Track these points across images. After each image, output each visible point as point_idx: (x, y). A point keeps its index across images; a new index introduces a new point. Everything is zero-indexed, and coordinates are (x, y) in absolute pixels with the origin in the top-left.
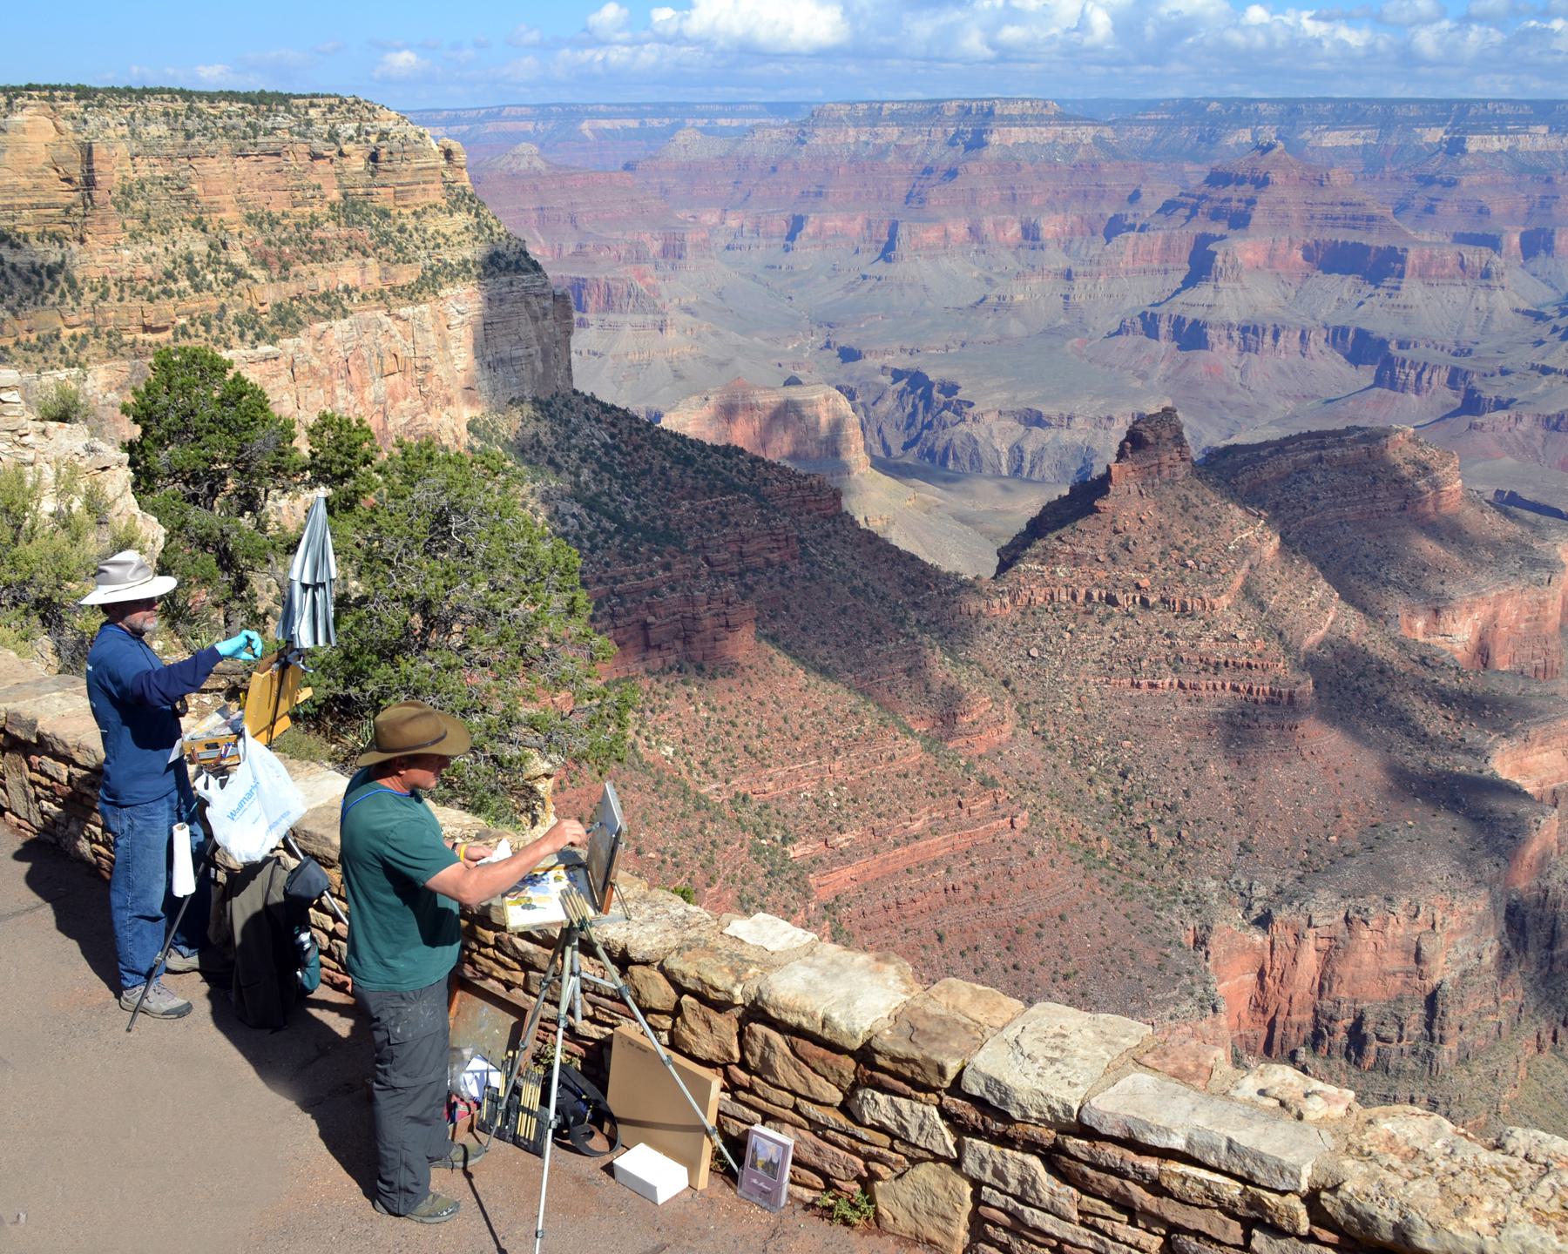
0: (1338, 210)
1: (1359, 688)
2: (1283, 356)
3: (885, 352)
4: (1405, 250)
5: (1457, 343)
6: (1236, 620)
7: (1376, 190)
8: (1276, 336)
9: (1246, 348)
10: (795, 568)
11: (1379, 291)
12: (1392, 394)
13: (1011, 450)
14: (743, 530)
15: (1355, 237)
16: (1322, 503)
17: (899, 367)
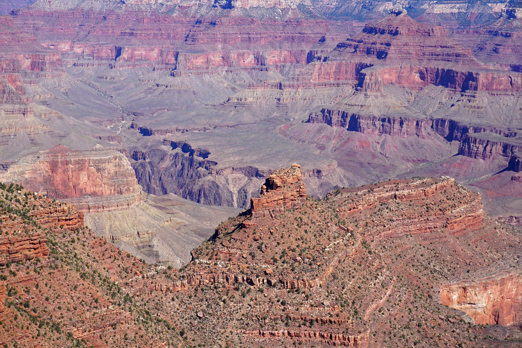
0: (439, 50)
1: (403, 336)
2: (406, 136)
3: (167, 131)
4: (477, 74)
5: (509, 129)
6: (324, 293)
7: (465, 39)
8: (401, 123)
9: (383, 131)
10: (44, 261)
11: (463, 98)
12: (469, 159)
13: (239, 192)
14: (10, 236)
15: (448, 66)
16: (395, 223)
17: (174, 140)
